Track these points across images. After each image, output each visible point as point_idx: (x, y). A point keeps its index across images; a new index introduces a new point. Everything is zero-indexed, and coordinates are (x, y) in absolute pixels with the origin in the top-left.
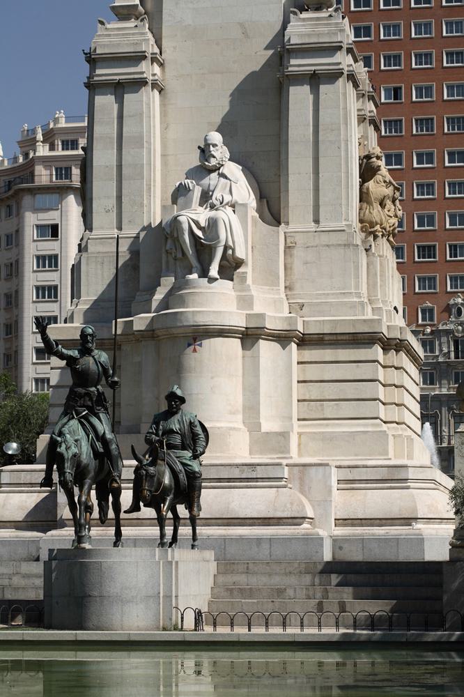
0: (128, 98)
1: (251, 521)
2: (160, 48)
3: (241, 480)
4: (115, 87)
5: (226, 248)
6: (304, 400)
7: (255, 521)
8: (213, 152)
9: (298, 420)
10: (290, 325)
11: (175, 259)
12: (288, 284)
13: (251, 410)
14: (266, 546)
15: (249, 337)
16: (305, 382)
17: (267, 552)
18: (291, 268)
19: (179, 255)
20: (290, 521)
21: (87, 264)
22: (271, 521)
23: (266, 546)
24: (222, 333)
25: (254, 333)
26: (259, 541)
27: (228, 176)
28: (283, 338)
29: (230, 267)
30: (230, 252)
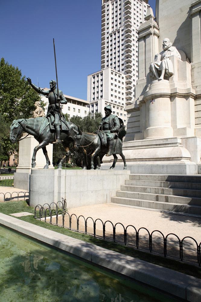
0: (147, 40)
1: (163, 159)
2: (158, 25)
3: (163, 144)
4: (144, 38)
5: (166, 70)
6: (197, 118)
7: (164, 159)
8: (165, 44)
9: (195, 125)
10: (188, 91)
11: (153, 78)
12: (192, 81)
13: (174, 121)
14: (165, 168)
15: (172, 97)
16: (197, 111)
17: (166, 170)
18: (193, 76)
19: (154, 76)
20: (176, 158)
21: (137, 88)
22: (170, 159)
23: (165, 168)
24: (162, 96)
25: (174, 95)
26: (163, 166)
27: (170, 50)
28: (186, 96)
29: (168, 76)
30: (167, 71)
